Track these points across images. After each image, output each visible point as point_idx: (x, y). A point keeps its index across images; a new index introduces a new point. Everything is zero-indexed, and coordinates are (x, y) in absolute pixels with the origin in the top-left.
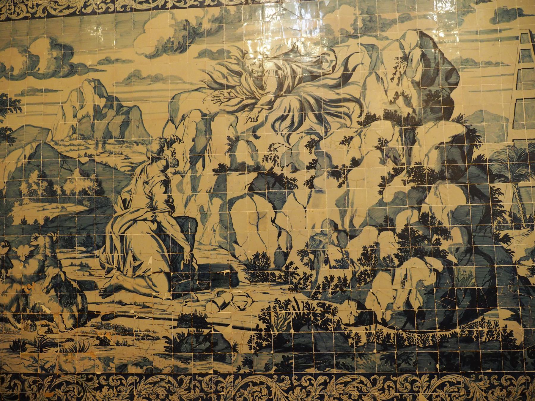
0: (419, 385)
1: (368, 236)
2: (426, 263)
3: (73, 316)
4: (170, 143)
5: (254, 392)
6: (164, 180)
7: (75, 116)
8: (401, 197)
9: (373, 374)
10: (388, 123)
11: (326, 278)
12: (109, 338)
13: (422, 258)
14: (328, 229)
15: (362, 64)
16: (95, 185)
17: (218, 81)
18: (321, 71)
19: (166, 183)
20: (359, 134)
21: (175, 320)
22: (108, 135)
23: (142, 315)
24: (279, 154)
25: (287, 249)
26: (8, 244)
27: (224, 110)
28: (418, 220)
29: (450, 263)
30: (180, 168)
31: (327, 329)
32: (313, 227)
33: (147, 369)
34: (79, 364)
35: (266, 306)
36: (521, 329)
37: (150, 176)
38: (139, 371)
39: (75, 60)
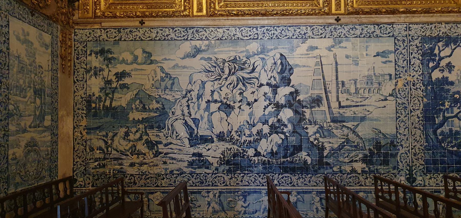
1: (259, 126)
3: (153, 153)
7: (153, 80)
8: (271, 113)
13: (277, 134)
14: (245, 123)
19: (188, 106)
22: (166, 88)
26: (128, 127)
29: (287, 136)
34: (156, 170)
36: (310, 159)
38: (178, 173)
39: (153, 58)
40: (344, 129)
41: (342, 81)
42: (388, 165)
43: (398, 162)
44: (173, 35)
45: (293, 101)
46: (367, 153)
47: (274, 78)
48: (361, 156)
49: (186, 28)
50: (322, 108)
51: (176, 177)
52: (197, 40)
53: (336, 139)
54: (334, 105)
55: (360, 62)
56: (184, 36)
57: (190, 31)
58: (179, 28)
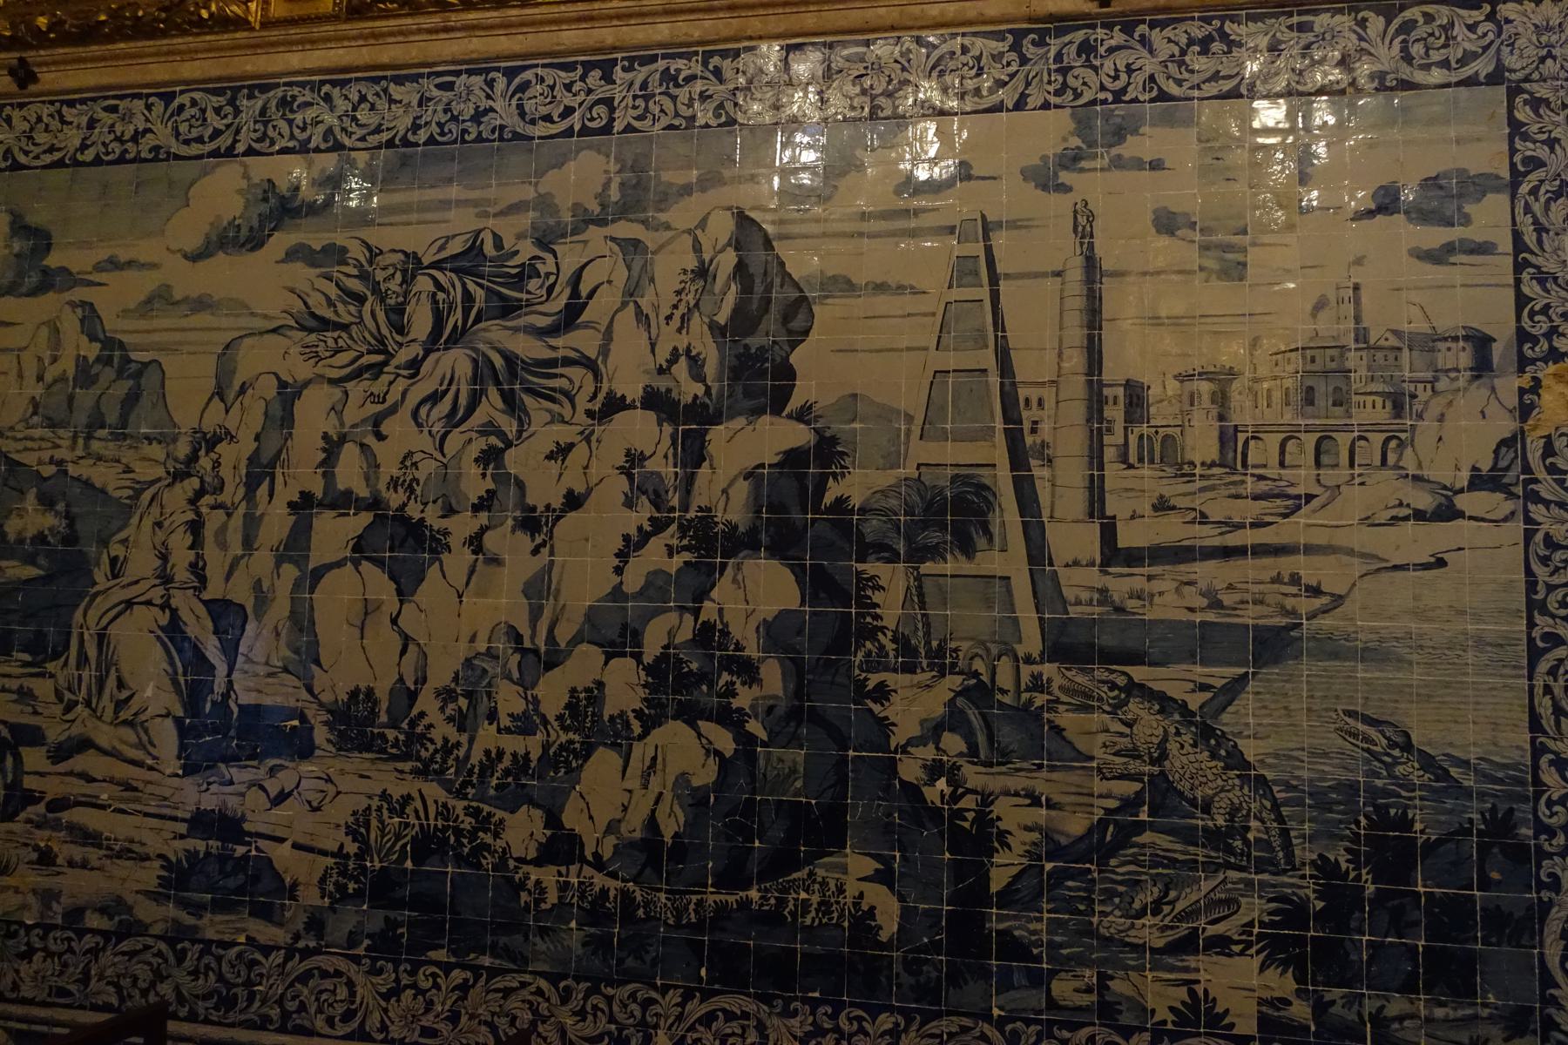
0: (660, 1010)
2: (700, 735)
4: (212, 442)
5: (321, 992)
6: (193, 521)
7: (40, 378)
9: (565, 977)
10: (652, 415)
11: (487, 753)
12: (56, 849)
14: (500, 646)
15: (609, 282)
16: (61, 525)
17: (318, 312)
18: (525, 296)
19: (196, 527)
20: (588, 440)
21: (184, 820)
23: (123, 806)
24: (421, 475)
25: (416, 683)
27: (322, 376)
28: (690, 636)
29: (751, 739)
30: (225, 498)
31: (479, 866)
32: (473, 639)
33: (121, 922)
35: (365, 802)
36: (894, 906)
37: (168, 511)
39: (53, 260)
40: (1135, 707)
41: (1128, 384)
42: (1464, 990)
43: (1548, 981)
44: (162, 134)
45: (798, 512)
46: (1309, 892)
47: (695, 363)
48: (1254, 908)
49: (231, 90)
50: (989, 562)
51: (95, 952)
52: (284, 151)
53: (1074, 778)
54: (1072, 539)
55: (1252, 256)
56: (217, 133)
57: (250, 107)
58: (197, 95)
